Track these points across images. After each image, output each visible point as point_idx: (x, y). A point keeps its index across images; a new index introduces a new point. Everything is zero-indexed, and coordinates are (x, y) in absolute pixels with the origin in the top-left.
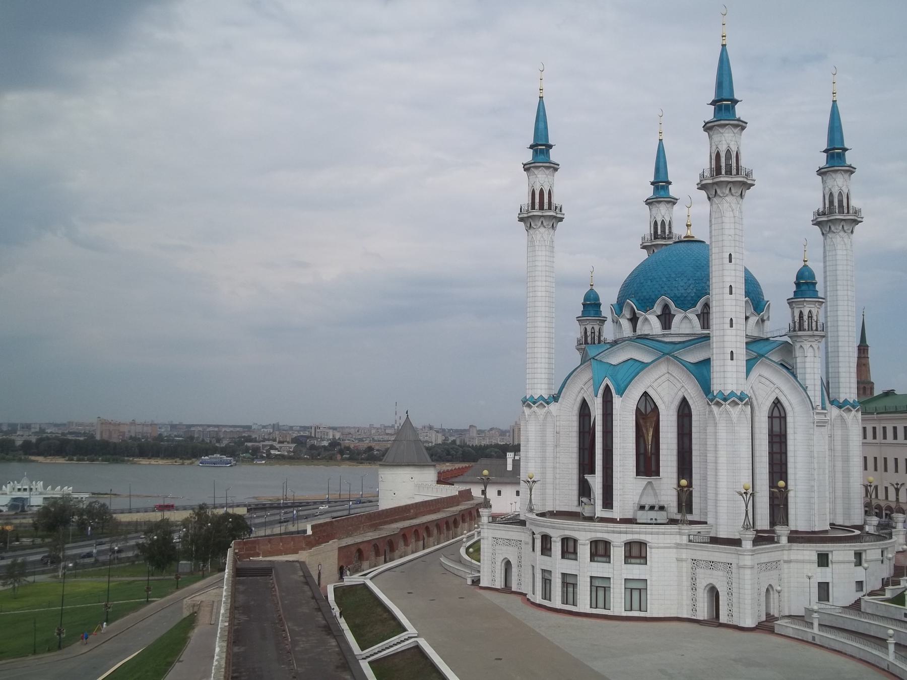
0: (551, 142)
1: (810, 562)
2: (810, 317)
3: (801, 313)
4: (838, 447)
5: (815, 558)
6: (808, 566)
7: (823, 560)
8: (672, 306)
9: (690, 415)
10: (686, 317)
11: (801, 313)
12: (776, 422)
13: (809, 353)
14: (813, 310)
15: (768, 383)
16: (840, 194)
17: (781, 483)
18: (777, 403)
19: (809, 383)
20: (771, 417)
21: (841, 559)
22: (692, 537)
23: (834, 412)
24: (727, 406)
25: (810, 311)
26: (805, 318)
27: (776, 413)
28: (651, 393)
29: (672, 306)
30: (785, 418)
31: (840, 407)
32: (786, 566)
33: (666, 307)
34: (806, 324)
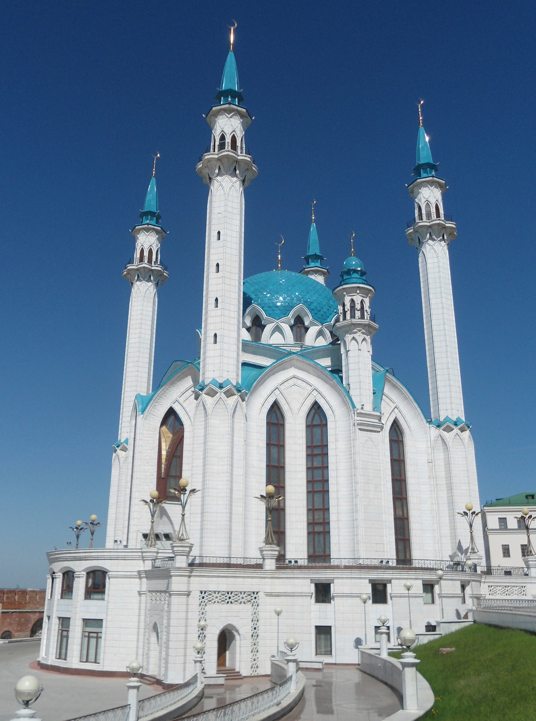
1: (301, 595)
4: (442, 473)
5: (312, 588)
6: (299, 601)
7: (323, 592)
13: (352, 346)
14: (354, 298)
15: (304, 384)
16: (428, 205)
17: (271, 488)
18: (316, 408)
21: (346, 590)
22: (158, 563)
23: (434, 432)
25: (352, 301)
28: (178, 409)
31: (439, 426)
32: (269, 600)
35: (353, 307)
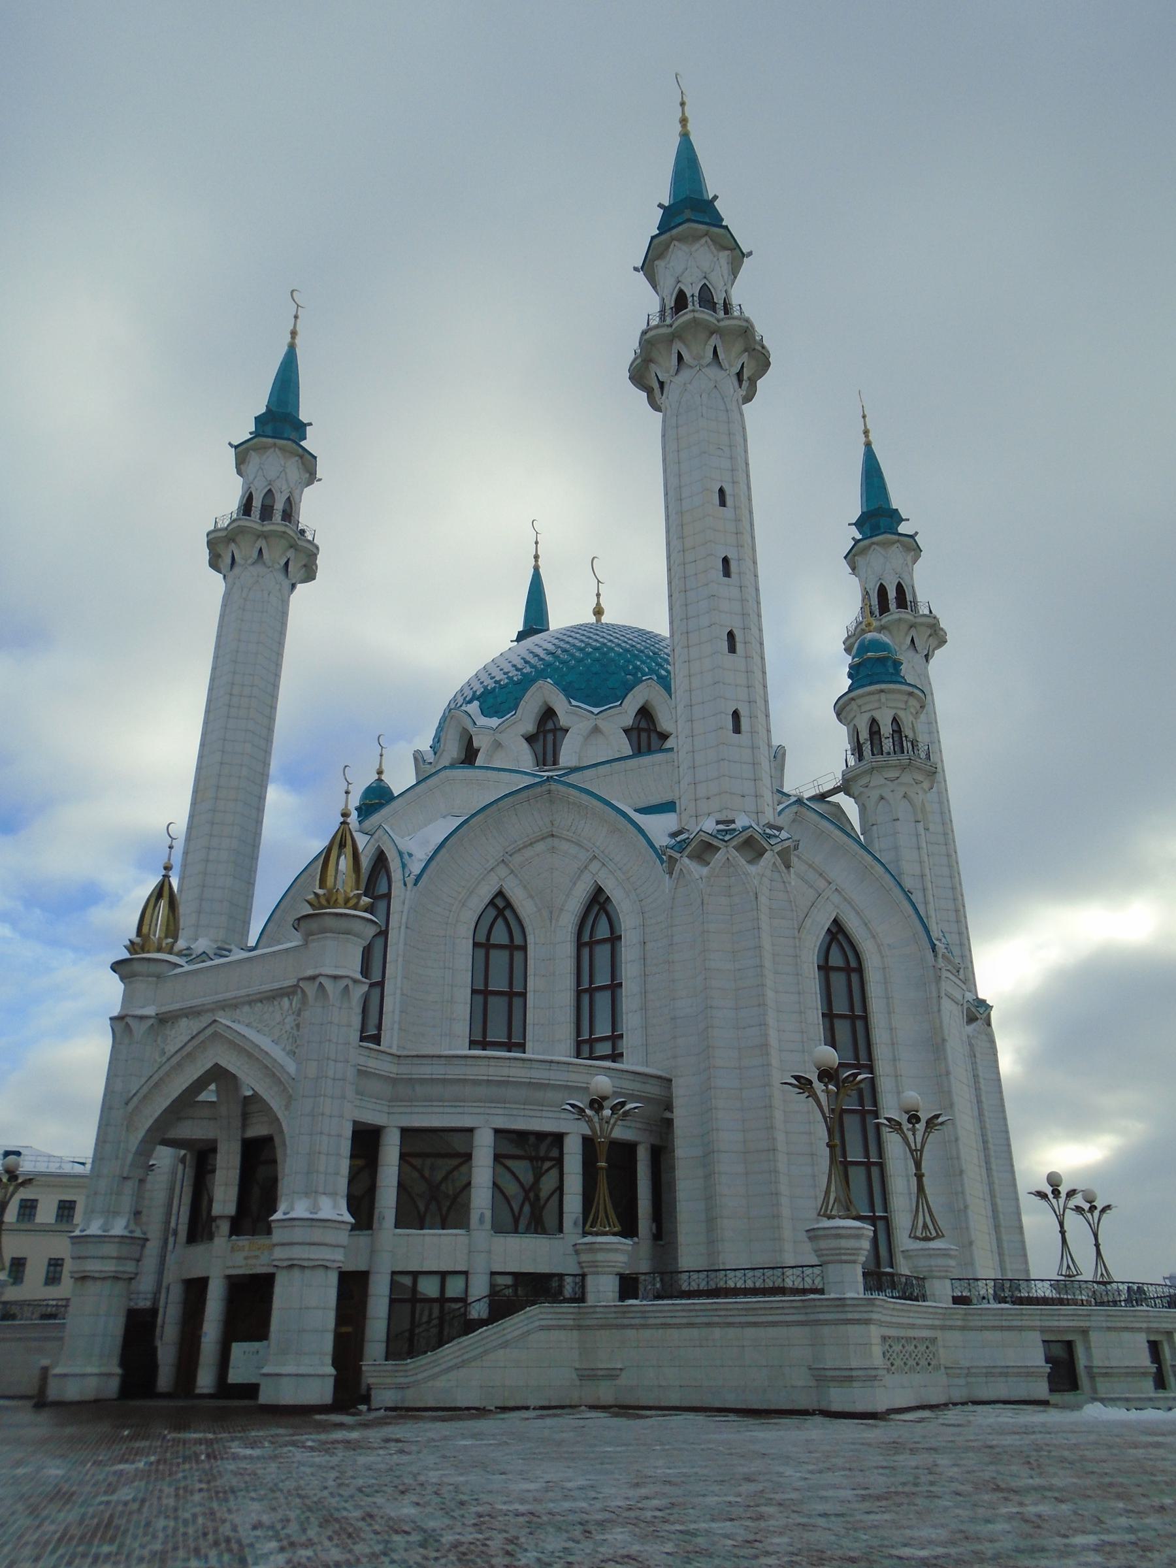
0: (303, 417)
2: (898, 730)
3: (874, 722)
5: (1037, 1358)
8: (560, 704)
9: (614, 939)
10: (596, 730)
11: (874, 722)
12: (838, 980)
14: (902, 714)
18: (837, 933)
19: (908, 883)
20: (825, 968)
24: (726, 853)
26: (886, 729)
27: (836, 959)
29: (560, 704)
30: (860, 970)
33: (549, 714)
34: (888, 745)
35: (898, 730)
